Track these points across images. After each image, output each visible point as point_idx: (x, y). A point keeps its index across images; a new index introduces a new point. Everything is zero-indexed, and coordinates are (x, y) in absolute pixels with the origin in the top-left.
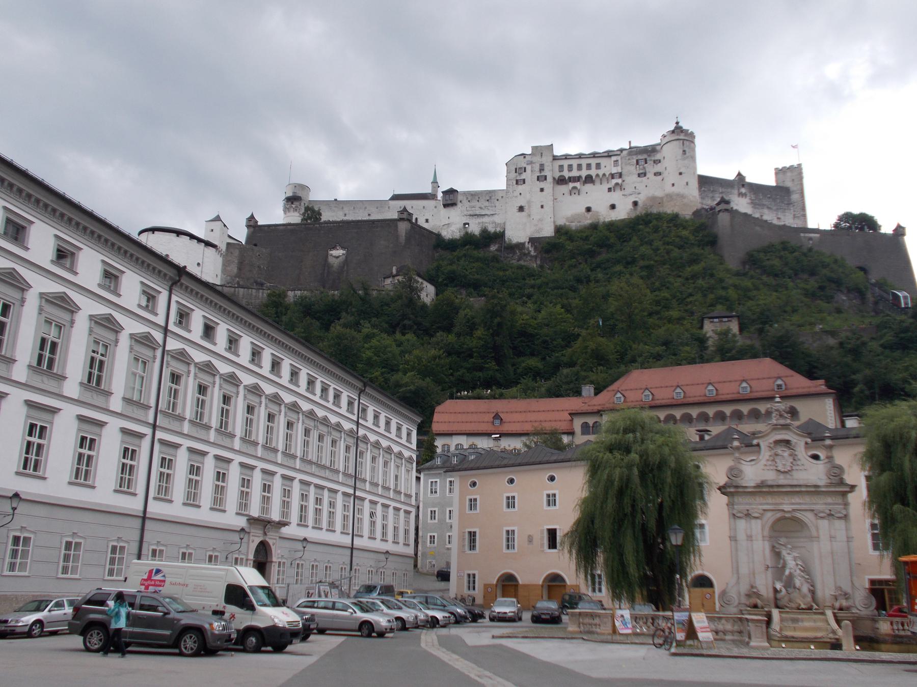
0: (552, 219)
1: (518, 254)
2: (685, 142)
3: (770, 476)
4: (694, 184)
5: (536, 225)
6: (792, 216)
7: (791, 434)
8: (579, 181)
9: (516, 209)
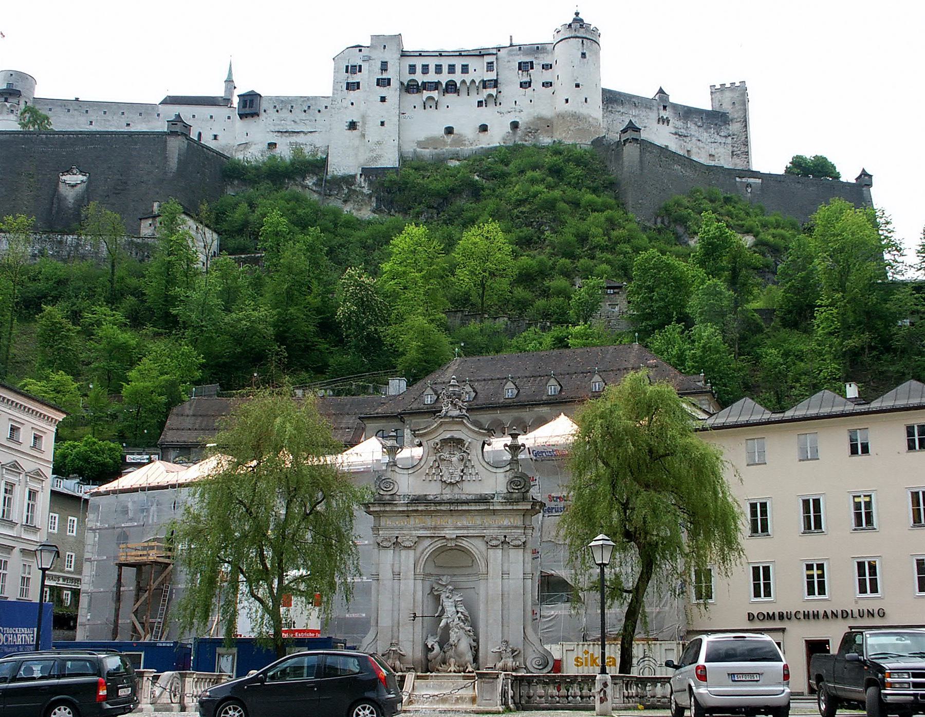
1: (346, 191)
3: (433, 490)
4: (597, 100)
5: (372, 150)
7: (465, 430)
8: (436, 89)
9: (345, 126)
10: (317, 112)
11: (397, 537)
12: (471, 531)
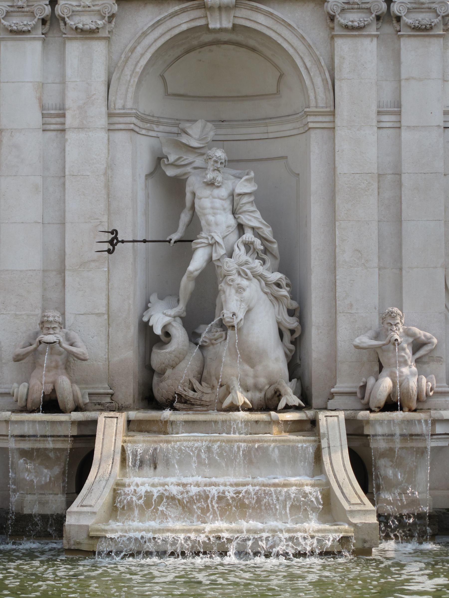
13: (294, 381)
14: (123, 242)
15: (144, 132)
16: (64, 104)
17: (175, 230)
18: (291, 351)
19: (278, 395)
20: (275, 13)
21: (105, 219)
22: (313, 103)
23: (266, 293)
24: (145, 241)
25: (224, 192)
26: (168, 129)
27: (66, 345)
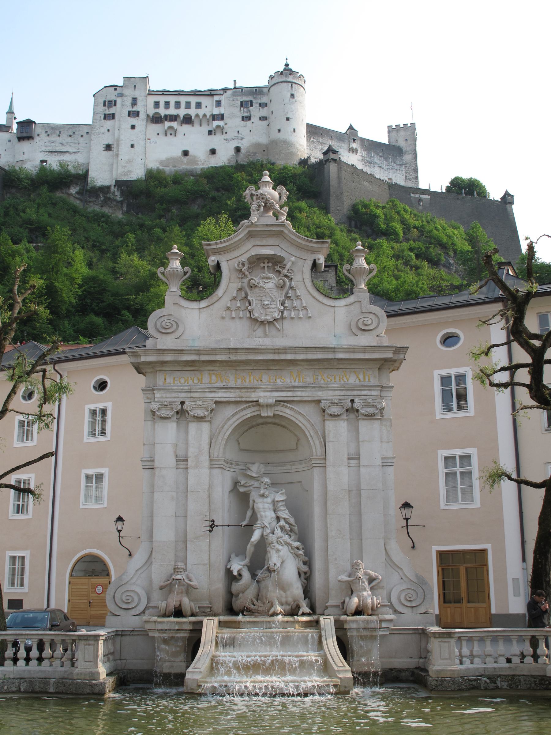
0: (143, 161)
1: (102, 198)
2: (294, 85)
5: (124, 167)
6: (404, 177)
7: (284, 245)
8: (176, 120)
9: (102, 148)
10: (80, 136)
11: (182, 403)
12: (299, 394)
13: (307, 599)
14: (217, 526)
15: (228, 469)
16: (187, 455)
17: (244, 520)
18: (305, 583)
19: (298, 607)
20: (295, 408)
21: (208, 514)
22: (315, 454)
23: (291, 553)
24: (228, 526)
25: (269, 500)
26: (240, 467)
27: (187, 581)
